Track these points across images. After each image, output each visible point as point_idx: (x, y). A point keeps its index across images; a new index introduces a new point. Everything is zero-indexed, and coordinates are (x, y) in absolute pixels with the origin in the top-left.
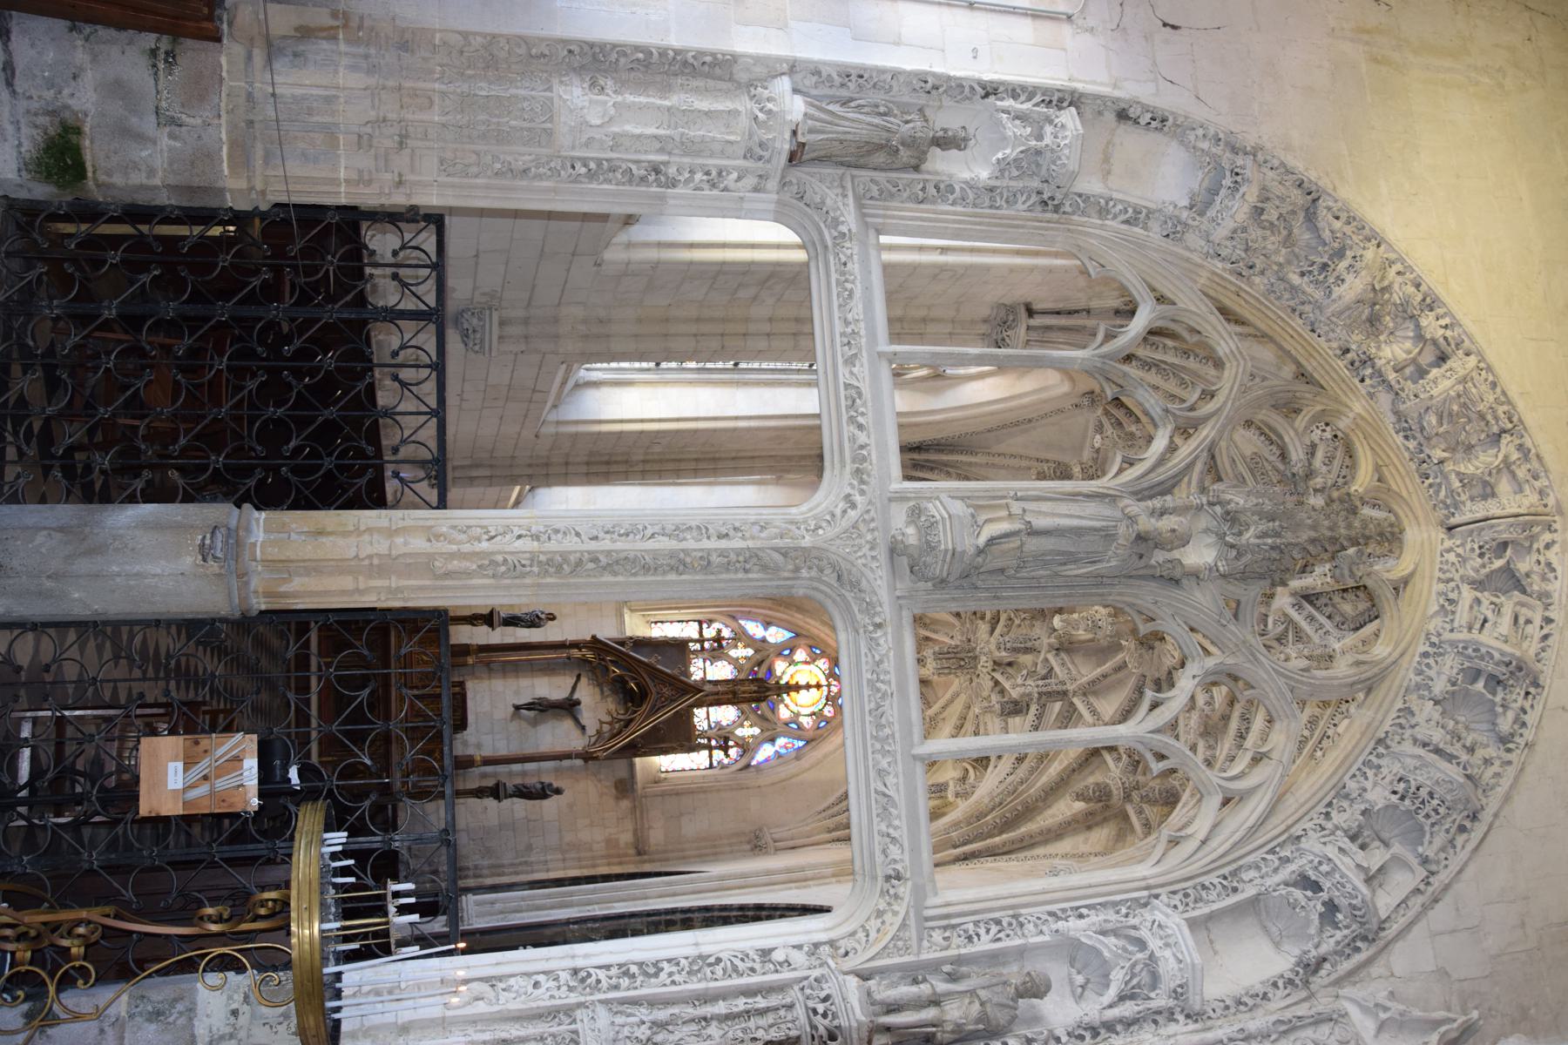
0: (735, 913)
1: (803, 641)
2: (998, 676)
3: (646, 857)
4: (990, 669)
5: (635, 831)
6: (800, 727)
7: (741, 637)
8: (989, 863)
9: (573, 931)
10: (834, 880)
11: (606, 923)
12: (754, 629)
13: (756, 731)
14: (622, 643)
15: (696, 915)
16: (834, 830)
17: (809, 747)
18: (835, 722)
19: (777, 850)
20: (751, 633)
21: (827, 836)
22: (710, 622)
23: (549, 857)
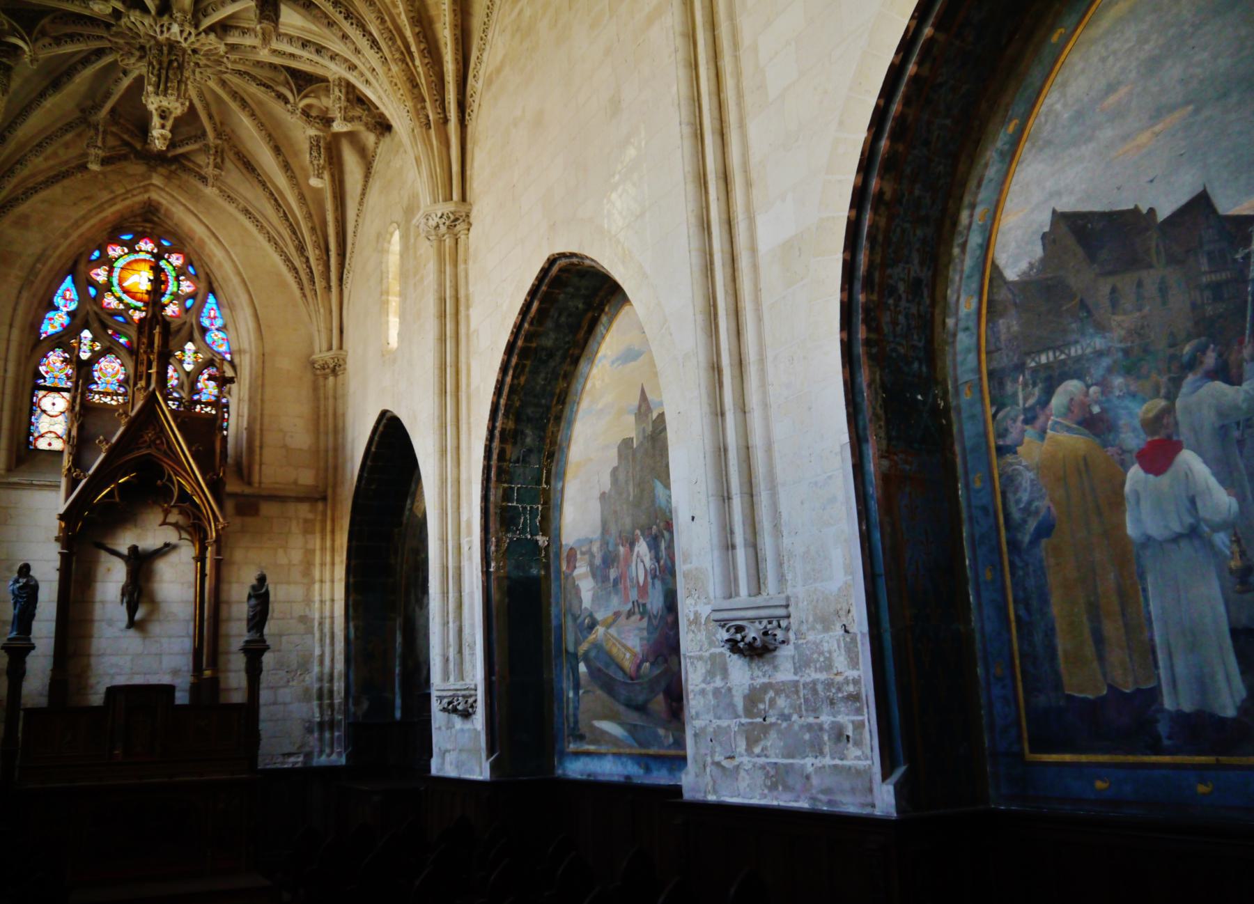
0: (509, 379)
1: (82, 267)
2: (206, 23)
3: (330, 491)
4: (193, 31)
5: (299, 499)
6: (193, 296)
7: (64, 340)
8: (476, 85)
9: (498, 568)
10: (461, 267)
11: (492, 530)
12: (54, 323)
13: (190, 346)
14: (73, 484)
15: (498, 424)
16: (328, 280)
17: (220, 292)
18: (194, 258)
19: (341, 347)
20: (59, 329)
21: (334, 290)
22: (39, 375)
23: (317, 598)
